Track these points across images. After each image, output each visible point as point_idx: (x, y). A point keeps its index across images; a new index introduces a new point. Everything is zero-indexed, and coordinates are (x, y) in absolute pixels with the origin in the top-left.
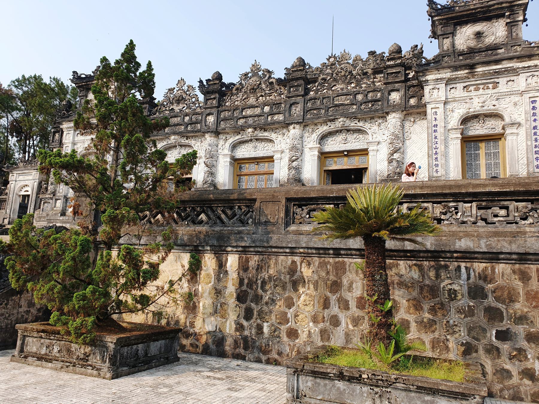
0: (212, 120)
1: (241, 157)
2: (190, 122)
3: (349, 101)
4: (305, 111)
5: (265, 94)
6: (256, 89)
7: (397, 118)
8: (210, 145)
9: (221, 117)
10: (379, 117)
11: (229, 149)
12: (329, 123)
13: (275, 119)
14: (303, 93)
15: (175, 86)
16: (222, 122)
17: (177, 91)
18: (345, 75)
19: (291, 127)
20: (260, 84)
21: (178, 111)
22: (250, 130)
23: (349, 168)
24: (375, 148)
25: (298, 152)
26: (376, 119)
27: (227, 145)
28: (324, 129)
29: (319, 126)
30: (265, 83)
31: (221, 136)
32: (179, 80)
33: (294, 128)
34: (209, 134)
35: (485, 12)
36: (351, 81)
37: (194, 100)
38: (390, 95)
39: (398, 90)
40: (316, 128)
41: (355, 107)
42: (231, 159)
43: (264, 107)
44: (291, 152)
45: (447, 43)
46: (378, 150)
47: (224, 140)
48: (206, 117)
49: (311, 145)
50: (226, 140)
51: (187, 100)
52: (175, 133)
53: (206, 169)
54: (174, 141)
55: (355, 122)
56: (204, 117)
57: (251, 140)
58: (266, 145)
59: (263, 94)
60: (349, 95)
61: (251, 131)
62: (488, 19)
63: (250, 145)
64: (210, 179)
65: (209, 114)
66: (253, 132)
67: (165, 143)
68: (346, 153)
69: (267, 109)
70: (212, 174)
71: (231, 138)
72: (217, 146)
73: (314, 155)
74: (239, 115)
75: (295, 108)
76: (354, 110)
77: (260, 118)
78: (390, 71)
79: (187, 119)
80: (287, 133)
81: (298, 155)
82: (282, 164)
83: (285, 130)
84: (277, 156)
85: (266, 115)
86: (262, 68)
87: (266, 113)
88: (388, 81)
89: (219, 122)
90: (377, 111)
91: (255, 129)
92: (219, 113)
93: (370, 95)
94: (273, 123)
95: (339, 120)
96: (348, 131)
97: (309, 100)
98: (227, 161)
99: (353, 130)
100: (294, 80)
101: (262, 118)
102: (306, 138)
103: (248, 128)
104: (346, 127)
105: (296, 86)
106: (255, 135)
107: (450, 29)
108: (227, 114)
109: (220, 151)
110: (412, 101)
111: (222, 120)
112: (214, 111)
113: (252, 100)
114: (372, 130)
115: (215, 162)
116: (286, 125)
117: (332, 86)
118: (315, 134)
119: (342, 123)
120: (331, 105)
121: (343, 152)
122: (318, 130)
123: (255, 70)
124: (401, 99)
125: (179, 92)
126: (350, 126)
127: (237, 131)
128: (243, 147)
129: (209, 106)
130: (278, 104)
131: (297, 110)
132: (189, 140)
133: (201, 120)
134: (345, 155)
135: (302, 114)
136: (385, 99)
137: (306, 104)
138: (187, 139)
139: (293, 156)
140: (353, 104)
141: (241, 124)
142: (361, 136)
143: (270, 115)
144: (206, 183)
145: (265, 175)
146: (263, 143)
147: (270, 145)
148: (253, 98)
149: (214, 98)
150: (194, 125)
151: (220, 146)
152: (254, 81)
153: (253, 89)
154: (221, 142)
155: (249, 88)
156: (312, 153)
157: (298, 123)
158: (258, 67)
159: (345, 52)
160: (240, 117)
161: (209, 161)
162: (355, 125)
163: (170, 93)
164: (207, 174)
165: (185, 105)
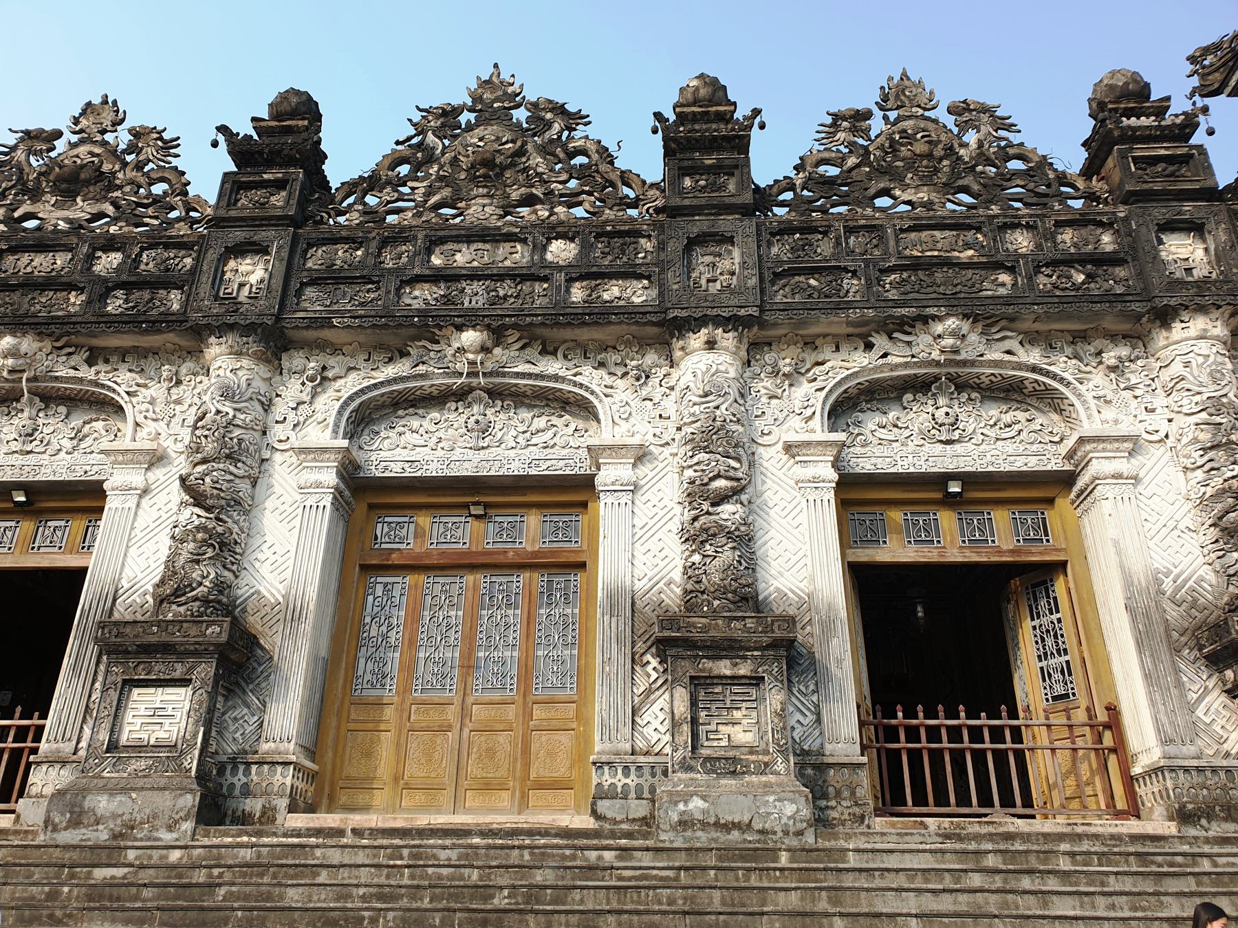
0: (253, 279)
1: (395, 470)
2: (124, 277)
3: (970, 252)
4: (768, 276)
5: (550, 193)
6: (504, 168)
7: (1217, 338)
8: (227, 393)
9: (309, 264)
10: (1115, 337)
11: (337, 425)
12: (880, 341)
13: (606, 296)
15: (64, 124)
16: (310, 292)
17: (73, 146)
18: (930, 156)
19: (696, 340)
20: (521, 152)
21: (62, 225)
22: (470, 337)
23: (975, 558)
24: (1121, 466)
25: (738, 460)
26: (1098, 343)
27: (328, 404)
29: (827, 353)
30: (544, 150)
31: (295, 360)
32: (89, 104)
33: (711, 345)
34: (230, 339)
36: (960, 182)
37: (158, 189)
38: (1161, 242)
39: (1196, 228)
40: (811, 358)
41: (1004, 278)
42: (340, 475)
43: (549, 240)
44: (702, 456)
46: (1136, 479)
47: (312, 379)
48: (223, 259)
49: (794, 430)
50: (322, 380)
51: (120, 187)
53: (191, 515)
54: (10, 362)
55: (1007, 345)
56: (212, 256)
57: (461, 395)
58: (541, 422)
59: (538, 192)
60: (969, 227)
61: (477, 344)
63: (452, 416)
64: (206, 575)
65: (239, 250)
66: (485, 349)
68: (955, 488)
69: (561, 251)
70: (222, 545)
71: (353, 376)
72: (267, 407)
73: (815, 480)
74: (411, 260)
75: (708, 259)
76: (1002, 291)
77: (526, 287)
78: (1141, 151)
79: (109, 262)
80: (664, 371)
81: (740, 475)
82: (644, 513)
83: (651, 358)
84: (610, 474)
85: (560, 277)
86: (531, 96)
87: (560, 268)
88: (1146, 186)
89: (295, 285)
90: (1109, 298)
91: (498, 335)
92: (297, 250)
94: (599, 315)
95: (939, 328)
96: (961, 386)
97: (781, 232)
98: (318, 485)
99: (978, 388)
100: (693, 150)
101: (539, 287)
102: (764, 400)
103: (460, 328)
104: (964, 363)
105: (709, 170)
106: (489, 366)
109: (278, 432)
111: (313, 282)
112: (278, 240)
114: (1091, 385)
115: (245, 486)
117: (872, 191)
118: (804, 389)
119: (948, 342)
120: (893, 262)
121: (943, 479)
122: (817, 370)
123: (497, 100)
125: (83, 150)
126: (982, 364)
127: (394, 342)
128: (415, 423)
129: (246, 213)
130: (621, 234)
132: (102, 367)
133: (195, 271)
134: (951, 501)
135: (753, 281)
137: (764, 244)
138: (90, 362)
139: (718, 476)
140: (999, 266)
141: (416, 304)
142: (1021, 416)
143: (581, 278)
144: (177, 593)
145: (525, 576)
146: (525, 414)
147: (565, 427)
148: (486, 201)
149: (279, 185)
150: (146, 295)
151: (281, 408)
152: (481, 139)
153: (488, 163)
154: (292, 390)
155: (465, 162)
156: (809, 472)
157: (731, 322)
158: (510, 90)
159: (908, 79)
160: (417, 271)
161: (213, 477)
162: (1007, 357)
163: (30, 152)
164: (191, 546)
165: (110, 210)
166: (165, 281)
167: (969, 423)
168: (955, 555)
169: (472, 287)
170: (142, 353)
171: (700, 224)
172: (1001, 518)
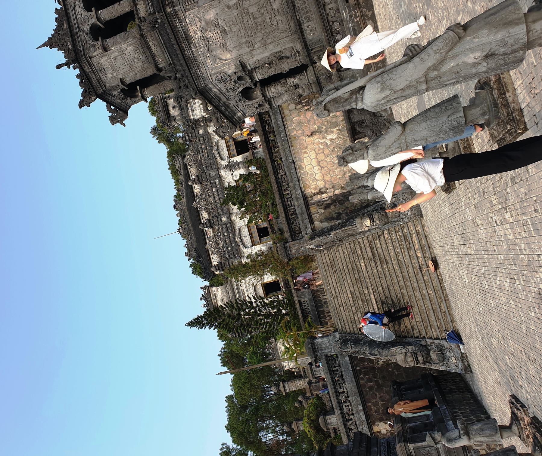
10: (210, 137)
12: (216, 158)
14: (204, 173)
28: (219, 159)
31: (231, 212)
35: (165, 107)
39: (198, 131)
45: (177, 118)
50: (232, 209)
52: (234, 239)
62: (168, 106)
65: (222, 221)
67: (241, 246)
78: (190, 137)
90: (208, 137)
93: (201, 142)
107: (172, 118)
108: (220, 210)
110: (202, 124)
113: (211, 200)
116: (220, 177)
121: (227, 149)
124: (201, 129)
131: (212, 173)
136: (202, 136)
166: (227, 227)
167: (222, 148)
168: (234, 147)
169: (220, 196)
170: (234, 227)
171: (208, 177)
172: (229, 144)
